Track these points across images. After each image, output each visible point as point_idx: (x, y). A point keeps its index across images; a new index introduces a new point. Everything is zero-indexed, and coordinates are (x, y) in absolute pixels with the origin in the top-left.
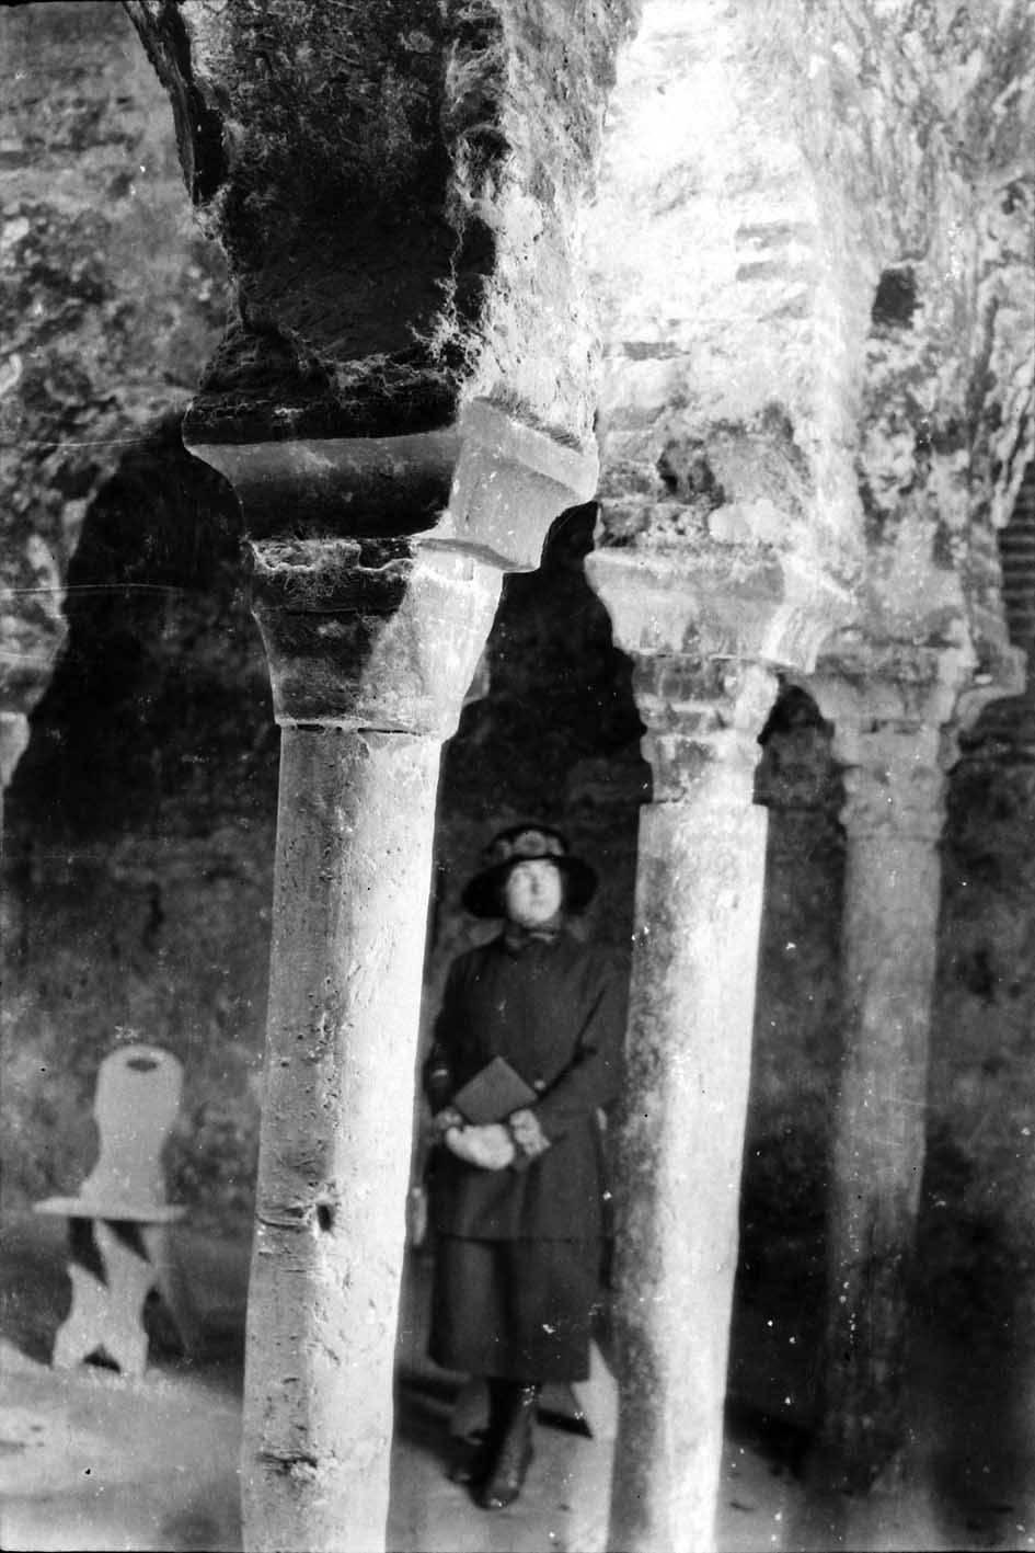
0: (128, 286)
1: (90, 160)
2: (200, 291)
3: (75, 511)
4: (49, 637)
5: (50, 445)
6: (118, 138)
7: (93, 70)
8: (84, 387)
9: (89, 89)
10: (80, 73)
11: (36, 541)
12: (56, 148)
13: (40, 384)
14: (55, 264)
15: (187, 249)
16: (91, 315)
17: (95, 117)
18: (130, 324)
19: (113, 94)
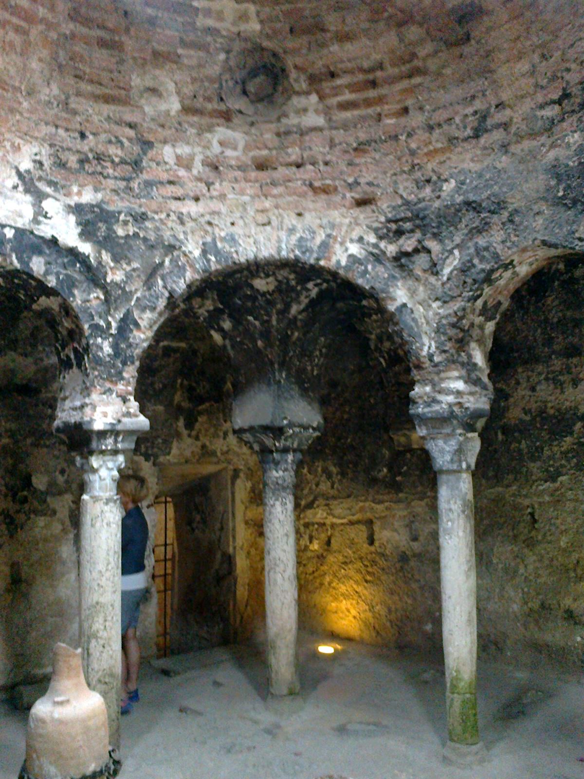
0: (515, 202)
1: (482, 141)
2: (558, 191)
3: (490, 327)
4: (484, 392)
5: (479, 292)
6: (498, 126)
7: (480, 95)
8: (496, 256)
9: (478, 105)
10: (473, 97)
11: (473, 345)
12: (466, 139)
13: (470, 261)
14: (472, 197)
15: (547, 171)
16: (495, 218)
17: (484, 118)
18: (517, 219)
19: (494, 103)
